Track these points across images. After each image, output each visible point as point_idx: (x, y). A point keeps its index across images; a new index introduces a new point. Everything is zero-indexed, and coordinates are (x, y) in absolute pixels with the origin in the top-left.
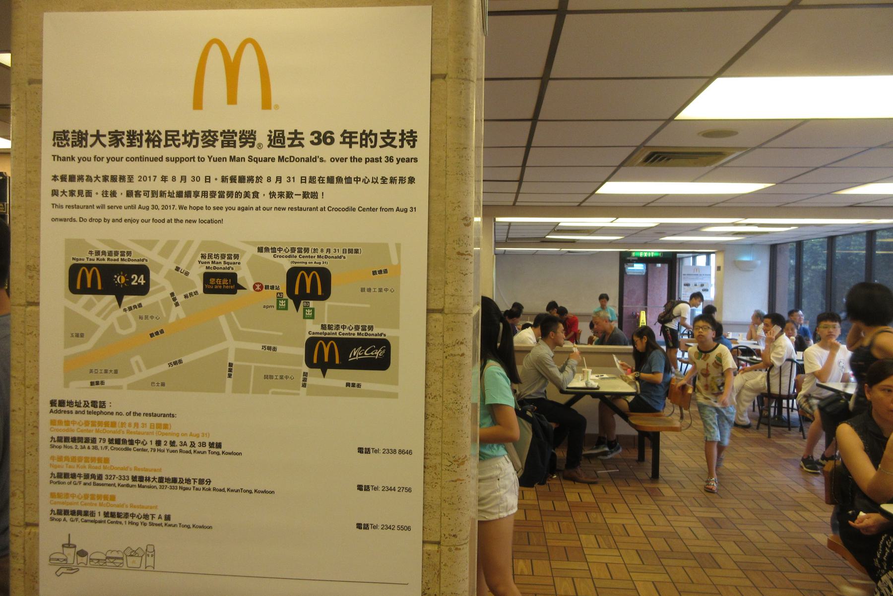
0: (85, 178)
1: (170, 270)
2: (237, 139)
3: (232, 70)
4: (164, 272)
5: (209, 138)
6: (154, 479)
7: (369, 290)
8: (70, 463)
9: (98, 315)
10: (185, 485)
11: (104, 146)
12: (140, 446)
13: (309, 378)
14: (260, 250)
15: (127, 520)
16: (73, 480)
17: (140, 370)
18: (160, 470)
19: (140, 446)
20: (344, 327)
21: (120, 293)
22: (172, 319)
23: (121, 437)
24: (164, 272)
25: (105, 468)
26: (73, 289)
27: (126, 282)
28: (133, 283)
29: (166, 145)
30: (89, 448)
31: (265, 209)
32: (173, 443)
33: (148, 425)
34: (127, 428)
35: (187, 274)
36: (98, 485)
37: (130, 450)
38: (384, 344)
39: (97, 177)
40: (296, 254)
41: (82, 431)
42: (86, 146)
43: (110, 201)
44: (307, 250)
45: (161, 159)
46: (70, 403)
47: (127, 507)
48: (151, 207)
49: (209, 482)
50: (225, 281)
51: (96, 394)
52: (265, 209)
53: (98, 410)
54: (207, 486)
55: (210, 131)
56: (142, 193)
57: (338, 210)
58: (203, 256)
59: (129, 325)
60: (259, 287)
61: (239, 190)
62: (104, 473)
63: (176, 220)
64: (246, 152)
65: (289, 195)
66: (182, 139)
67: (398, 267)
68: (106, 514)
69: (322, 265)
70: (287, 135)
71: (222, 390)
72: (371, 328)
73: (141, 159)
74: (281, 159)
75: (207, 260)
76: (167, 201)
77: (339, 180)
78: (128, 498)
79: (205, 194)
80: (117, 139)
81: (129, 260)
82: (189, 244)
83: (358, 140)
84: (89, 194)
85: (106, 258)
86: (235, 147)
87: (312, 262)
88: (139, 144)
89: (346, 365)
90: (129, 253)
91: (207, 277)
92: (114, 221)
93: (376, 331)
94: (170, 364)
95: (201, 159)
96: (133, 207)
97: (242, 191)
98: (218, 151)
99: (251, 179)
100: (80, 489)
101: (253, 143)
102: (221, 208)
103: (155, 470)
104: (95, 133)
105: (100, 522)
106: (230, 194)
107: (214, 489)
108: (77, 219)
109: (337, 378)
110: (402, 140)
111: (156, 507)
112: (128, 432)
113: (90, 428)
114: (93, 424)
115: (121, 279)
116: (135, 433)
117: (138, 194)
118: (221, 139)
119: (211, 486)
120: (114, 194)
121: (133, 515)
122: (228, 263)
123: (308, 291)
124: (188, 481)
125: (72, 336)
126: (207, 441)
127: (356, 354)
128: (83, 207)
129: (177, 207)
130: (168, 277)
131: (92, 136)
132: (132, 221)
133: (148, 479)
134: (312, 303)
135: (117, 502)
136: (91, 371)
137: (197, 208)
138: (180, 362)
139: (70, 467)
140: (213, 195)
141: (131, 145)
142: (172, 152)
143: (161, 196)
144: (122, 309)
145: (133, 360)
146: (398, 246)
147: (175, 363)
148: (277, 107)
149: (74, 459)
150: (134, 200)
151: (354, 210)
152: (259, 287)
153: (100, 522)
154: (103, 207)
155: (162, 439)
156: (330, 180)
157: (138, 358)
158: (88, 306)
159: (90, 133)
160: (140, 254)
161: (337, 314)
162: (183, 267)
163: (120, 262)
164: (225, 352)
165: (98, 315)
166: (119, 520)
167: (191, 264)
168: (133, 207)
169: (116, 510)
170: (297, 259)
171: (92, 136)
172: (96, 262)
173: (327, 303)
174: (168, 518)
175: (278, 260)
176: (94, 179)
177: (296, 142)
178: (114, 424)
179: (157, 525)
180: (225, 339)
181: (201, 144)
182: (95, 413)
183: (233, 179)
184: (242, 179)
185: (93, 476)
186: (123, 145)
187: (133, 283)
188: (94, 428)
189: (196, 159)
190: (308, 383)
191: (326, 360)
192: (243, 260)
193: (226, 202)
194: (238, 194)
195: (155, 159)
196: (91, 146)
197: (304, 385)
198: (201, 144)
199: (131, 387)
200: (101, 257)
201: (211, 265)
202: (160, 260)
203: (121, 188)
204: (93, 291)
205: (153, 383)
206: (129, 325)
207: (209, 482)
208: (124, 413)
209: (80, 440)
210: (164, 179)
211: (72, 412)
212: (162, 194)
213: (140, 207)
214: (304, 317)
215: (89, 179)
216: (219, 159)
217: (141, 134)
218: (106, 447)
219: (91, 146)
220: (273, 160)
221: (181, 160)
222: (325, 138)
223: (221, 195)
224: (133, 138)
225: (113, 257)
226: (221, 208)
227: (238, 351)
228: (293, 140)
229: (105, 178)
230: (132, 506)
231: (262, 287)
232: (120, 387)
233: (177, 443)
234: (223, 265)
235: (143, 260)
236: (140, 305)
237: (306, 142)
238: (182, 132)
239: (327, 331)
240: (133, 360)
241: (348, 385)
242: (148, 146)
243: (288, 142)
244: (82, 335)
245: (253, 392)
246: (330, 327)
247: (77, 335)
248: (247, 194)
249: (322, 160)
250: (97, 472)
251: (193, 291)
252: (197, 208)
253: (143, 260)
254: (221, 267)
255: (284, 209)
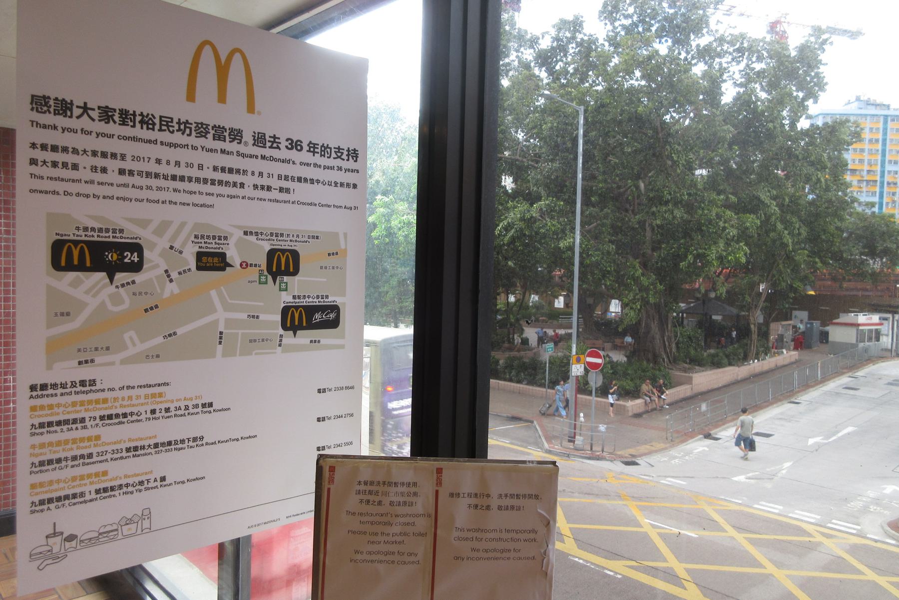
0: (70, 150)
1: (164, 249)
2: (226, 134)
3: (223, 71)
4: (158, 250)
5: (202, 130)
6: (149, 446)
7: (326, 268)
8: (55, 449)
9: (87, 292)
10: (180, 446)
11: (93, 120)
12: (135, 418)
13: (284, 339)
14: (246, 233)
15: (121, 491)
16: (58, 466)
17: (134, 345)
18: (155, 437)
19: (135, 418)
20: (309, 297)
21: (111, 271)
22: (167, 294)
23: (114, 412)
24: (158, 250)
25: (95, 446)
26: (56, 265)
27: (118, 259)
28: (126, 260)
29: (161, 130)
30: (77, 429)
31: (249, 198)
32: (167, 410)
33: (143, 397)
34: (121, 402)
35: (181, 252)
36: (88, 464)
37: (123, 423)
38: (335, 309)
39: (85, 151)
40: (274, 238)
41: (68, 413)
42: (71, 117)
43: (99, 177)
44: (282, 235)
45: (155, 142)
46: (54, 386)
47: (121, 478)
48: (144, 187)
49: (202, 438)
50: (216, 260)
51: (86, 373)
52: (249, 198)
53: (88, 388)
54: (201, 443)
55: (202, 124)
56: (136, 173)
57: (304, 204)
58: (196, 237)
59: (122, 302)
60: (244, 265)
61: (227, 179)
62: (94, 450)
63: (171, 202)
64: (233, 147)
65: (269, 188)
66: (176, 127)
67: (345, 250)
68: (98, 492)
69: (293, 248)
70: (268, 138)
71: (213, 355)
72: (327, 297)
73: (134, 139)
74: (263, 157)
75: (199, 240)
76: (161, 183)
77: (306, 180)
78: (120, 470)
79: (198, 180)
80: (107, 115)
81: (121, 237)
82: (183, 225)
83: (319, 150)
84: (75, 167)
85: (95, 234)
86: (225, 141)
87: (285, 245)
88: (132, 124)
89: (311, 326)
90: (121, 231)
91: (200, 256)
92: (104, 197)
93: (330, 299)
94: (165, 337)
95: (194, 148)
96: (125, 185)
97: (231, 181)
98: (209, 142)
99: (238, 171)
100: (68, 473)
101: (241, 140)
102: (213, 194)
103: (150, 438)
104: (82, 105)
105: (91, 501)
106: (220, 183)
107: (207, 444)
108: (61, 193)
109: (304, 337)
110: (348, 155)
111: (151, 472)
112: (121, 406)
113: (78, 408)
114: (82, 403)
115: (112, 257)
116: (128, 406)
117: (131, 173)
118: (212, 132)
119: (204, 442)
120: (104, 170)
121: (127, 485)
122: (219, 244)
123: (283, 268)
124: (182, 441)
125: (56, 315)
126: (200, 402)
127: (318, 317)
128: (69, 180)
129: (171, 189)
130: (162, 255)
131: (78, 107)
132: (124, 199)
133: (143, 448)
134: (286, 278)
135: (110, 476)
136: (79, 350)
137: (191, 193)
138: (175, 334)
139: (55, 452)
140: (205, 181)
141: (123, 123)
142: (166, 136)
143: (155, 177)
144: (114, 286)
145: (126, 336)
146: (345, 235)
147: (170, 335)
148: (259, 113)
149: (59, 443)
150: (126, 179)
151: (315, 205)
152: (244, 265)
153: (91, 501)
154: (92, 182)
155: (157, 407)
156: (299, 180)
157: (132, 333)
158: (75, 284)
159: (76, 103)
160: (132, 232)
161: (304, 287)
162: (177, 245)
163: (111, 239)
164: (217, 321)
165: (87, 292)
166: (113, 493)
167: (184, 244)
168: (125, 185)
169: (108, 485)
170: (275, 242)
171: (78, 107)
172: (83, 238)
173: (297, 278)
174: (163, 479)
175: (260, 242)
176: (81, 153)
177: (275, 145)
178: (105, 401)
179: (152, 488)
180: (215, 311)
181: (194, 133)
182: (84, 392)
183: (223, 170)
184: (231, 171)
185: (82, 457)
186: (115, 122)
187: (126, 260)
188: (83, 408)
189: (190, 147)
190: (283, 343)
191: (297, 323)
192: (232, 241)
193: (217, 189)
194: (227, 183)
195: (150, 141)
196: (78, 117)
197: (280, 345)
198: (194, 133)
199: (123, 362)
200: (89, 233)
201: (203, 245)
202: (154, 239)
203: (114, 165)
204: (81, 267)
205: (148, 356)
206: (122, 302)
207: (202, 438)
208: (117, 388)
209: (66, 422)
210: (158, 161)
211: (56, 395)
212: (157, 176)
213: (133, 186)
214: (280, 290)
215: (75, 151)
216: (211, 150)
217: (134, 114)
218: (97, 425)
219: (78, 117)
220: (257, 157)
221: (176, 146)
222: (296, 145)
223: (213, 182)
224: (126, 117)
225: (104, 234)
226: (213, 194)
227: (227, 321)
228: (273, 142)
229: (94, 154)
230: (126, 476)
231: (247, 265)
232: (113, 364)
233: (172, 409)
234: (214, 246)
235: (136, 238)
236: (133, 282)
237: (282, 146)
238: (175, 120)
239: (297, 300)
240: (126, 336)
241: (311, 341)
242: (142, 128)
243: (268, 144)
244: (68, 314)
245: (240, 355)
246: (299, 297)
247: (62, 314)
248: (235, 185)
249: (294, 163)
250: (85, 452)
251: (186, 268)
252: (191, 193)
253: (136, 238)
254: (212, 247)
255: (265, 200)
